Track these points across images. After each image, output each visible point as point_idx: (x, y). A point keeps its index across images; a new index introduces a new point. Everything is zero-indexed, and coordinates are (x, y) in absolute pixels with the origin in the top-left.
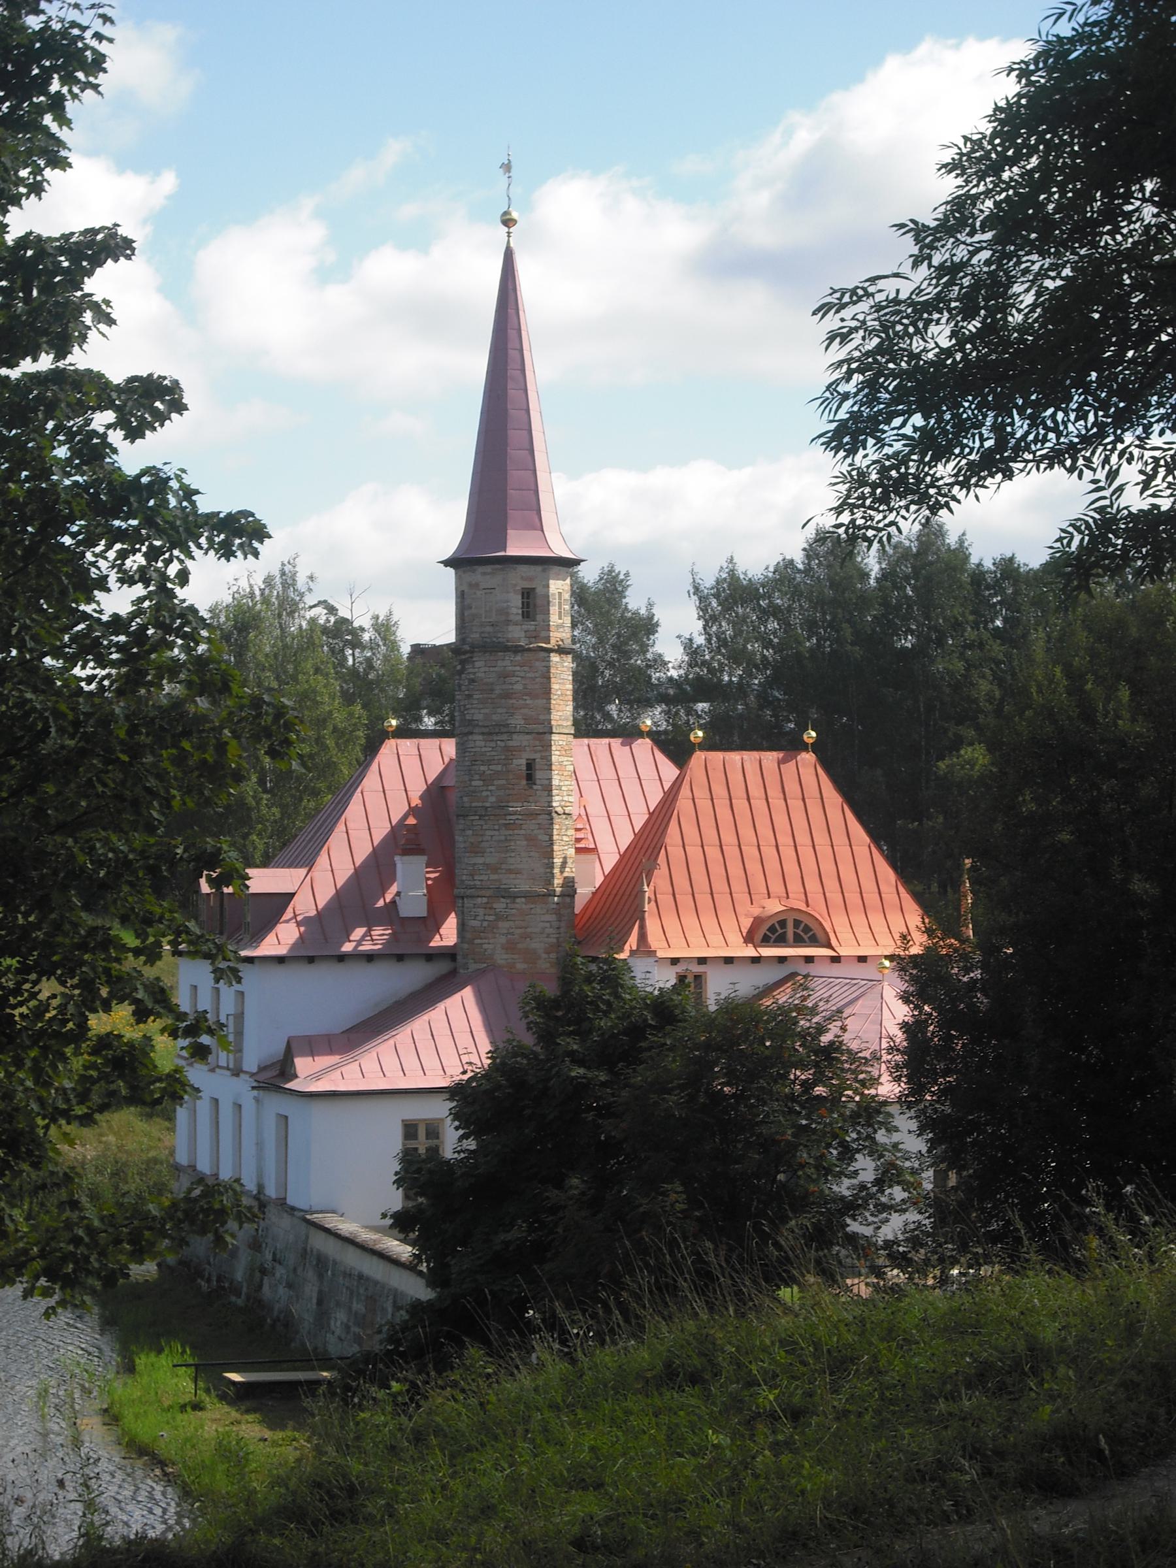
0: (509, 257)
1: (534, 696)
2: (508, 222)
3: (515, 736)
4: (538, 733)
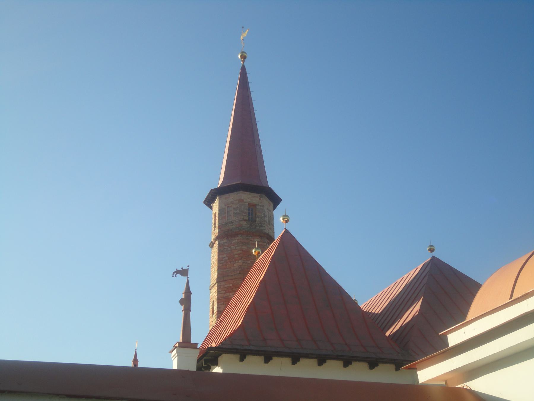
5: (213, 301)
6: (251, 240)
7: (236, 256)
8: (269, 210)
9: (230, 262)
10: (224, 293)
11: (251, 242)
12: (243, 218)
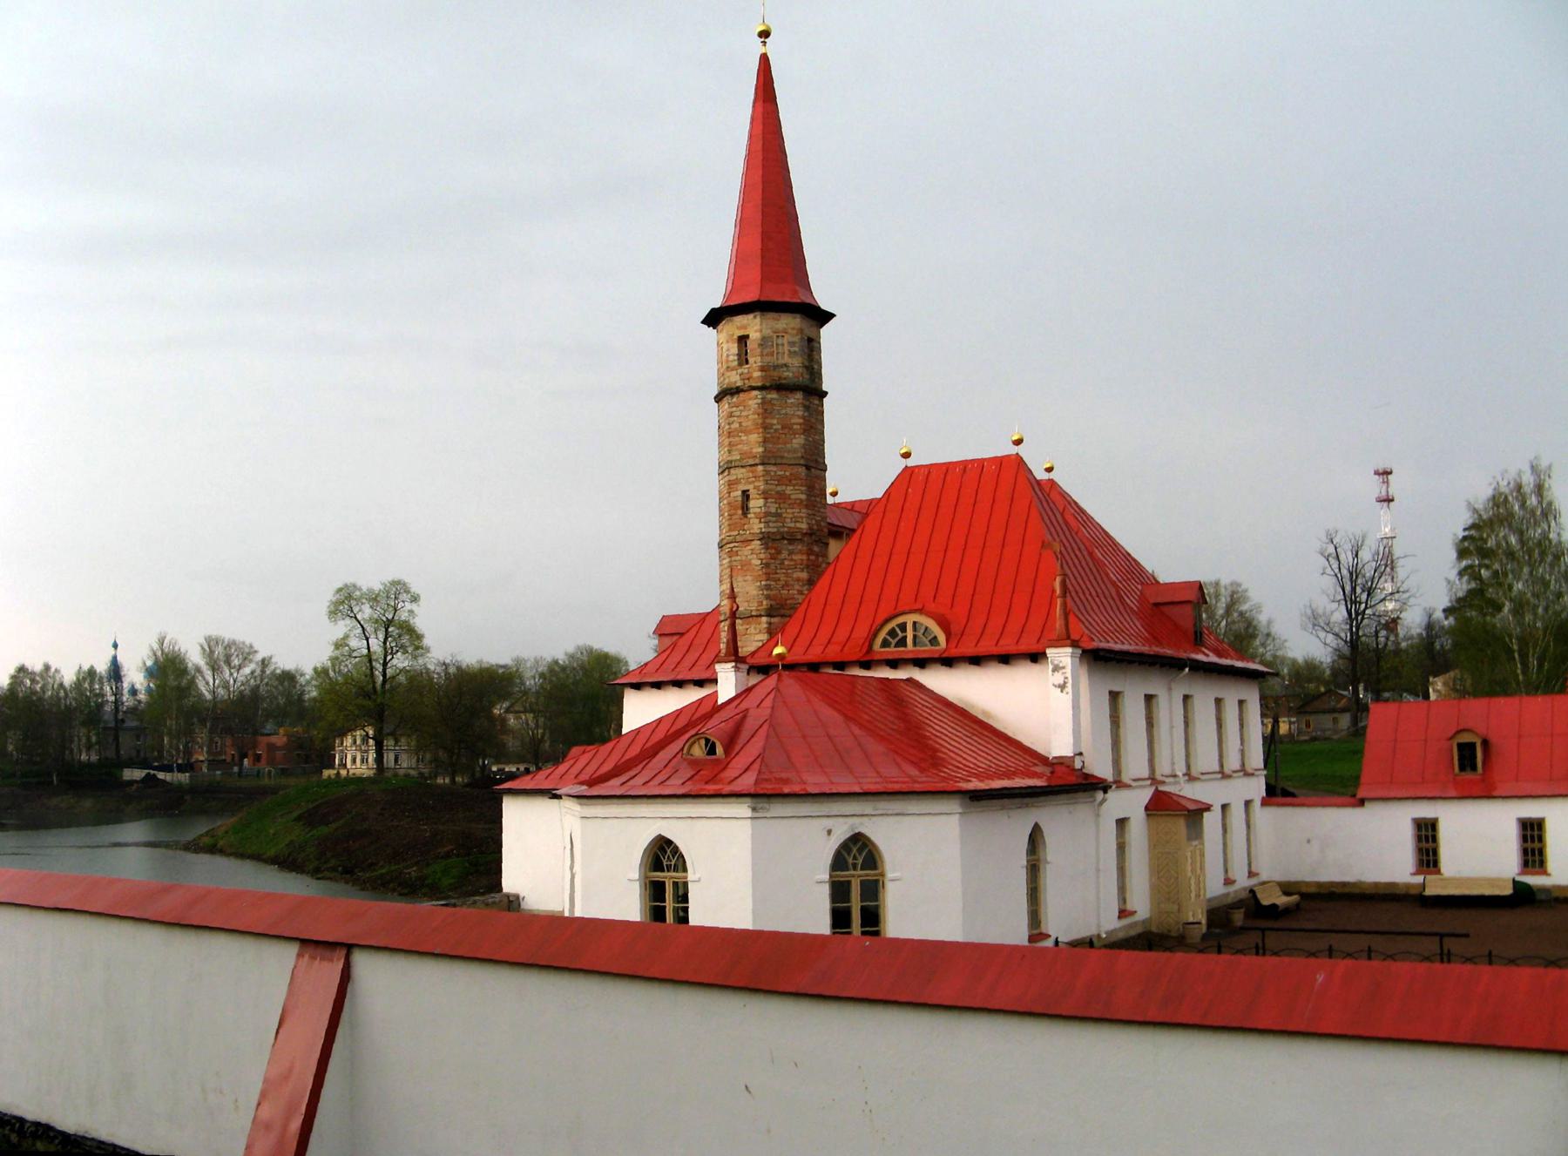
1: (747, 432)
3: (732, 471)
4: (751, 466)
5: (746, 495)
7: (795, 427)
9: (785, 434)
10: (777, 485)
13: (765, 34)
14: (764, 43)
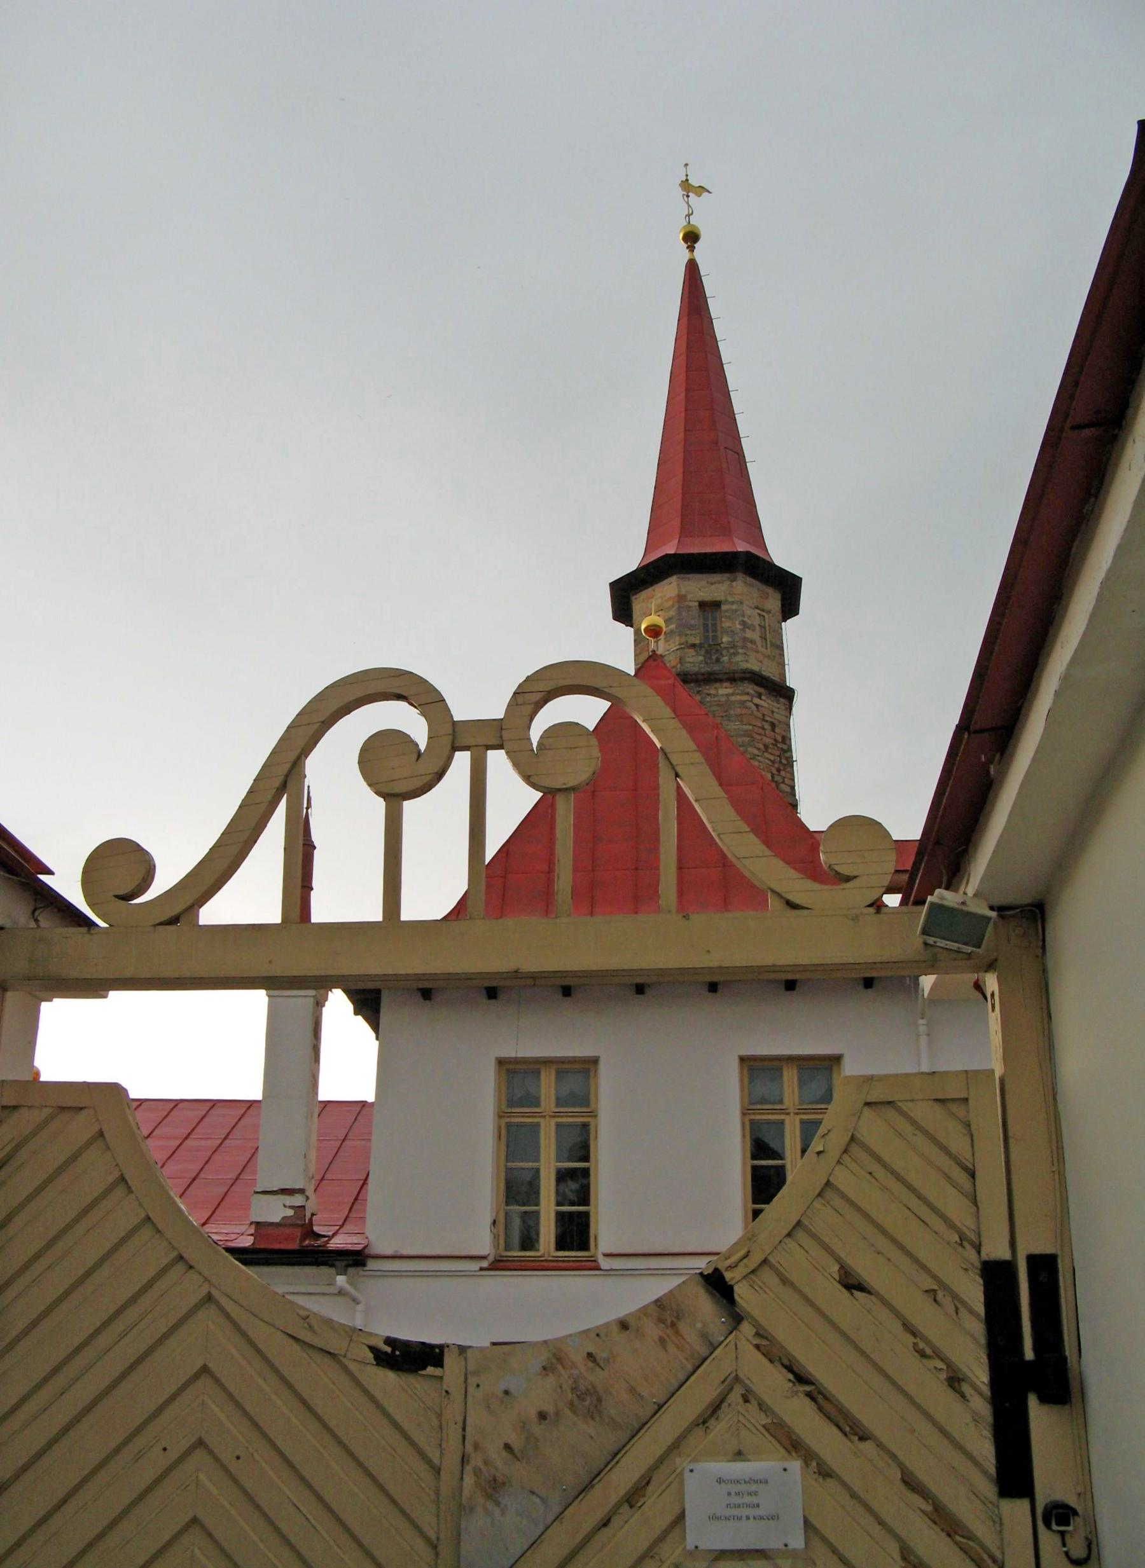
0: (692, 269)
2: (691, 238)
6: (709, 695)
8: (761, 610)
11: (708, 699)
12: (687, 642)
13: (691, 238)
14: (691, 248)
